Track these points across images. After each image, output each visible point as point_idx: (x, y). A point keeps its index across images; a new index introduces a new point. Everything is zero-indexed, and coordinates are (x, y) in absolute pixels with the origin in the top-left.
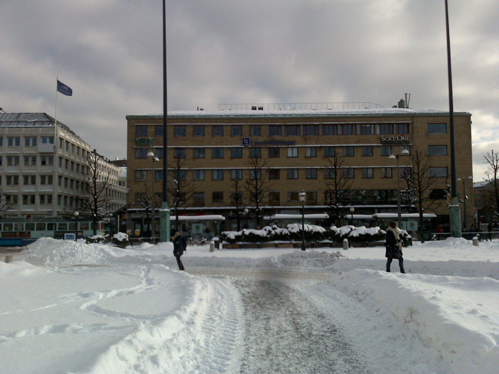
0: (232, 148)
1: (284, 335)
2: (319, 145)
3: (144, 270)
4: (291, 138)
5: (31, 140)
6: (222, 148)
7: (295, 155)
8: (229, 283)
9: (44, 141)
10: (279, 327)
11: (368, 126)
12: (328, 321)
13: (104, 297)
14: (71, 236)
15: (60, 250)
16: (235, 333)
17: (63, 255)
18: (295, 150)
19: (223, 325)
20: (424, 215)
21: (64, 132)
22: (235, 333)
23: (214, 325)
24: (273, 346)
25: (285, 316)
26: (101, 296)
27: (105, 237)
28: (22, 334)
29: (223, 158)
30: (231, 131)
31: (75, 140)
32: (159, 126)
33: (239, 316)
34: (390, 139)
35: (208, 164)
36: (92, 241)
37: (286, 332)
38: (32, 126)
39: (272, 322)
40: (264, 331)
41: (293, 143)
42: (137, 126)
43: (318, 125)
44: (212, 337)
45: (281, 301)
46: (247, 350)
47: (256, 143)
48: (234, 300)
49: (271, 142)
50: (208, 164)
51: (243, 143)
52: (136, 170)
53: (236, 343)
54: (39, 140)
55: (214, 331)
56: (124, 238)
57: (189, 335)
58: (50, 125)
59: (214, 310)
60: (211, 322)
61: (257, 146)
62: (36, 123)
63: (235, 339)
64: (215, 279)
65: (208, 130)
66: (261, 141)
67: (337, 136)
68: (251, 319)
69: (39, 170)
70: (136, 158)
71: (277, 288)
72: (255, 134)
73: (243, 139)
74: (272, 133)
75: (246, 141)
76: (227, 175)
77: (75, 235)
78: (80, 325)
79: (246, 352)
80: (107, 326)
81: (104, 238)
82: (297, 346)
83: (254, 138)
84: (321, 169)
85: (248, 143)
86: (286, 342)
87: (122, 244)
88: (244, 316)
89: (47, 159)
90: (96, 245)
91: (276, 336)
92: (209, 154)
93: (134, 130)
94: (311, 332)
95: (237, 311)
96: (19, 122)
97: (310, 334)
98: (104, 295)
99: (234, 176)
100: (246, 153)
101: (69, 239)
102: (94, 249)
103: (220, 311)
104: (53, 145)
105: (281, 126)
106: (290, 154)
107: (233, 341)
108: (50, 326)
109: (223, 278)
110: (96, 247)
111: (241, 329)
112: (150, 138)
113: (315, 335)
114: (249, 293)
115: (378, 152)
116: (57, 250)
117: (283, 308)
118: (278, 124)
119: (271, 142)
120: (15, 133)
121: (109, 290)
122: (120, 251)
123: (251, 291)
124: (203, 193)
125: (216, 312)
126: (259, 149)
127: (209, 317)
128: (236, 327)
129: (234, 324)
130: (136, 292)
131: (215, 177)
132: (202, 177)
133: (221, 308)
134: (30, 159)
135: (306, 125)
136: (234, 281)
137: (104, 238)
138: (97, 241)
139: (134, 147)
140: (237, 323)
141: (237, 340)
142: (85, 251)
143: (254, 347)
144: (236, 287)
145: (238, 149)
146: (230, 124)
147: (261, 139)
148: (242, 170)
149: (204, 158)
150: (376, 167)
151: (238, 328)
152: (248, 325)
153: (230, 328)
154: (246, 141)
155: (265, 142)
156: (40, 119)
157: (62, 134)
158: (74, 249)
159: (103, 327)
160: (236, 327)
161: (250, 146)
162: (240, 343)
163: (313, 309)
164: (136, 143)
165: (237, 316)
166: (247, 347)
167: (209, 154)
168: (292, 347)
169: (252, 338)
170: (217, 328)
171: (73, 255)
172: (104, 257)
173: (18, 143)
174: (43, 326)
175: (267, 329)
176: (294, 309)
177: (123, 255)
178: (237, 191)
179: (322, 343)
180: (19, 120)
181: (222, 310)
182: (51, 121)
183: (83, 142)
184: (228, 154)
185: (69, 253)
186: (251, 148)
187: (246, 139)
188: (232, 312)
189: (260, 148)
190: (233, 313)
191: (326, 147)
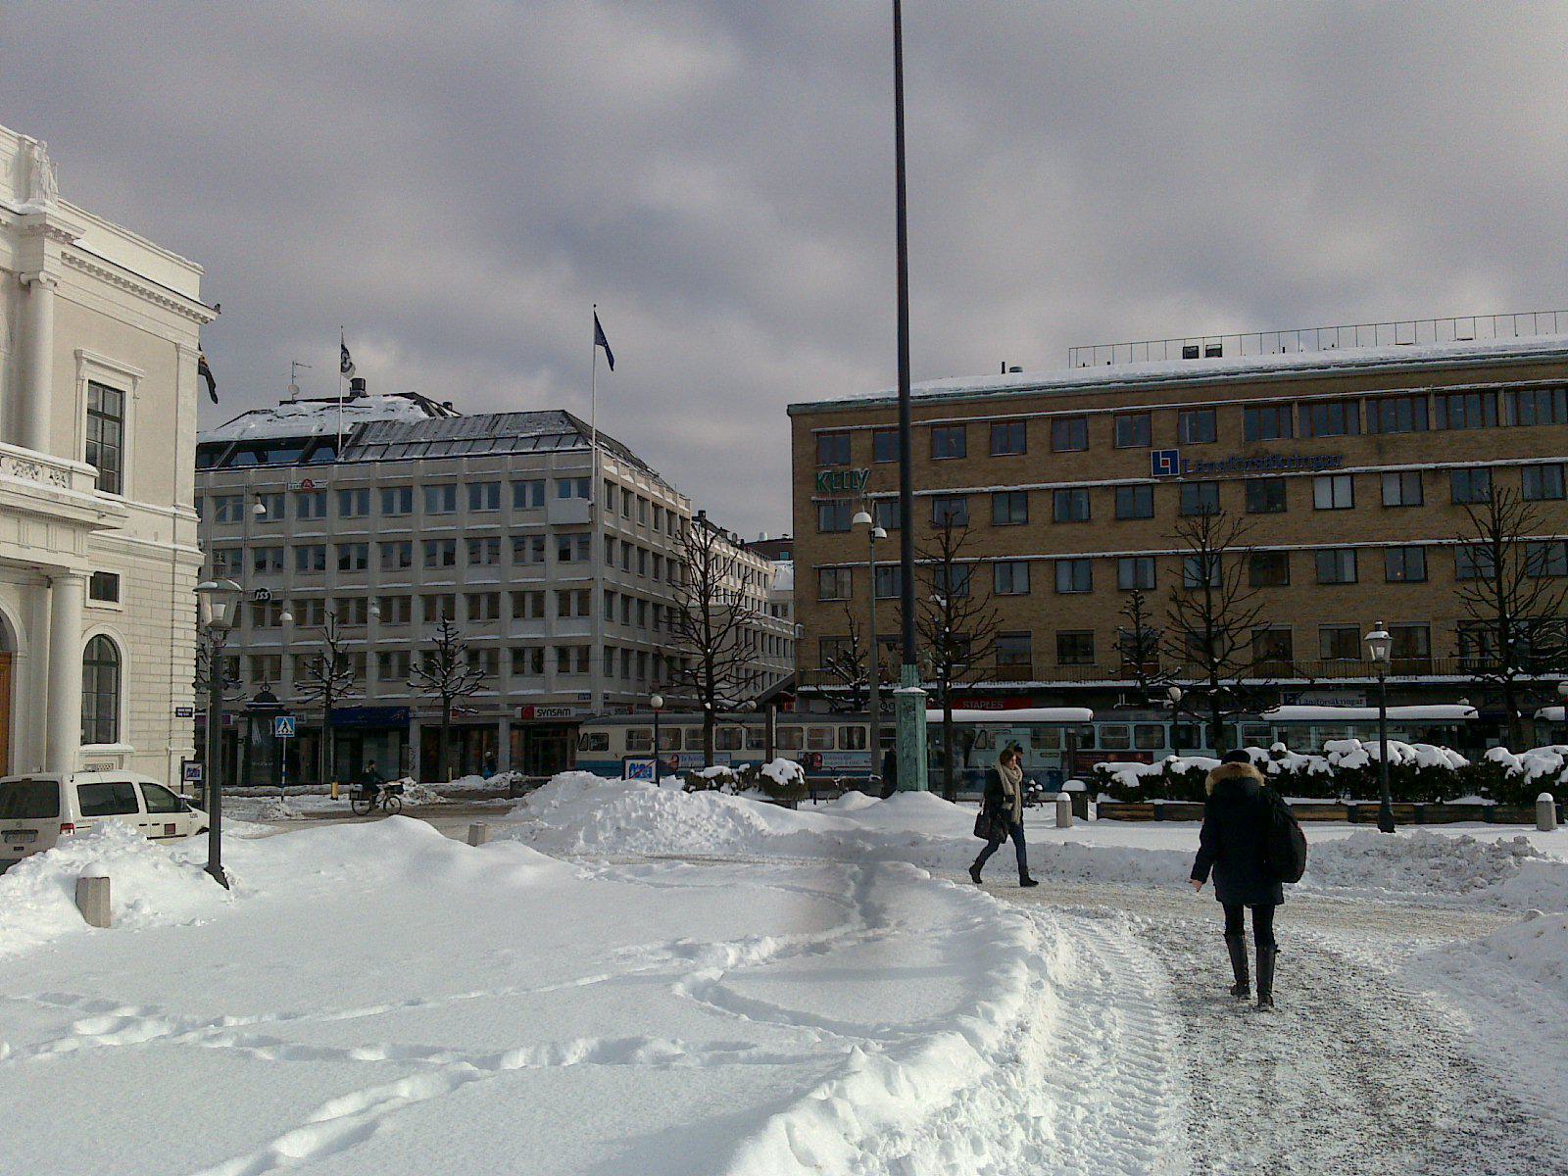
0: (1117, 487)
1: (1329, 1124)
2: (1432, 466)
3: (853, 877)
4: (1325, 445)
5: (530, 491)
6: (1086, 488)
8: (1126, 933)
9: (564, 493)
10: (1309, 1094)
12: (1490, 1084)
13: (740, 960)
14: (643, 766)
15: (615, 808)
16: (1155, 1104)
17: (623, 824)
18: (1343, 487)
19: (1114, 1073)
21: (615, 464)
22: (1155, 1104)
23: (1085, 1070)
24: (1290, 1158)
25: (1329, 1057)
26: (732, 955)
27: (738, 773)
28: (517, 1061)
29: (1088, 520)
30: (1114, 429)
31: (648, 485)
33: (1166, 1046)
35: (1039, 542)
36: (701, 784)
37: (1334, 1111)
38: (531, 450)
39: (1281, 1072)
40: (1256, 1103)
41: (1335, 460)
42: (819, 434)
43: (1425, 395)
44: (1080, 1113)
45: (1312, 1004)
46: (1199, 1164)
47: (1200, 467)
48: (1147, 994)
49: (1255, 463)
50: (1039, 542)
51: (1157, 469)
52: (820, 569)
53: (1162, 1136)
54: (551, 490)
55: (1085, 1092)
56: (791, 778)
57: (1004, 1099)
58: (580, 446)
59: (1082, 1024)
60: (1073, 1061)
61: (1204, 478)
62: (541, 439)
63: (1158, 1125)
64: (1081, 920)
65: (1038, 434)
66: (1218, 460)
67: (1493, 431)
68: (1209, 1060)
69: (554, 574)
70: (820, 533)
71: (1293, 959)
72: (1196, 437)
73: (1156, 455)
74: (1254, 433)
76: (1103, 577)
77: (654, 765)
78: (674, 1042)
79: (1198, 1170)
80: (754, 1051)
81: (736, 777)
82: (1378, 1164)
83: (1191, 452)
85: (1174, 470)
86: (1338, 1149)
87: (785, 795)
88: (1185, 1048)
89: (572, 542)
90: (715, 795)
91: (1300, 1125)
92: (1040, 510)
93: (811, 449)
94: (1428, 1118)
95: (1160, 1029)
96: (496, 439)
97: (1425, 1126)
98: (741, 950)
99: (1127, 579)
100: (1166, 501)
101: (637, 776)
102: (706, 807)
103: (1100, 1025)
104: (590, 502)
105: (1289, 404)
106: (1323, 500)
107: (1153, 1131)
108: (594, 1042)
109: (1106, 916)
110: (712, 803)
111: (1176, 1093)
112: (859, 470)
113: (1444, 1133)
114: (1196, 971)
116: (606, 812)
117: (1319, 1029)
118: (1276, 399)
119: (1255, 463)
120: (487, 470)
121: (756, 936)
122: (783, 816)
123: (1203, 966)
125: (1086, 1028)
126: (1212, 487)
127: (1068, 1044)
128: (1158, 1083)
129: (1151, 1074)
130: (834, 946)
131: (1064, 583)
132: (1020, 583)
133: (1105, 1016)
134: (527, 545)
135: (1379, 398)
136: (1144, 926)
137: (736, 777)
138: (714, 784)
139: (813, 498)
140: (1163, 1070)
141: (1163, 1129)
142: (682, 815)
143: (1224, 1157)
144: (1153, 949)
145: (1138, 491)
146: (1112, 410)
147: (1217, 453)
148: (1154, 557)
151: (1164, 1086)
152: (1199, 1078)
153: (1139, 1087)
155: (1232, 464)
156: (552, 430)
157: (610, 468)
158: (652, 808)
159: (742, 1054)
160: (1158, 1083)
162: (1174, 1139)
163: (1433, 1037)
164: (819, 487)
165: (1160, 1046)
166: (1200, 1153)
167: (1040, 510)
168: (1360, 1167)
169: (1217, 1125)
170: (1094, 1084)
171: (648, 824)
172: (735, 832)
173: (494, 502)
174: (574, 1040)
175: (1268, 1100)
176: (1363, 1034)
177: (790, 829)
178: (1138, 629)
179: (1474, 1162)
180: (496, 432)
181: (1107, 1024)
182: (582, 432)
183: (669, 489)
184: (1104, 508)
185: (640, 818)
186: (1182, 483)
187: (1165, 454)
188: (1142, 1033)
189: (1217, 482)
190: (1148, 1036)
191: (1454, 468)
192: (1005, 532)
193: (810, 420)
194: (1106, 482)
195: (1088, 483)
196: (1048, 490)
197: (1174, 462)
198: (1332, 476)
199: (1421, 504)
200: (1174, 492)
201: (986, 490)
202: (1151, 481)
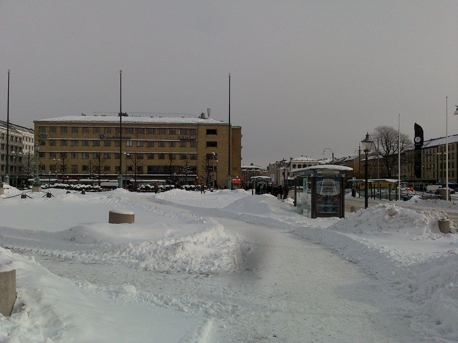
0: (94, 140)
2: (145, 140)
4: (129, 135)
7: (131, 145)
11: (173, 129)
18: (131, 142)
20: (137, 181)
32: (52, 127)
34: (185, 138)
41: (129, 138)
42: (39, 127)
43: (144, 128)
47: (108, 138)
50: (80, 149)
51: (100, 138)
65: (80, 130)
67: (155, 135)
75: (102, 136)
84: (145, 153)
85: (103, 138)
100: (102, 143)
106: (128, 145)
115: (178, 145)
124: (77, 166)
135: (138, 128)
147: (111, 136)
149: (77, 146)
150: (177, 153)
154: (102, 136)
155: (113, 137)
161: (104, 139)
167: (80, 143)
192: (74, 147)
193: (38, 124)
194: (91, 139)
195: (88, 139)
196: (81, 140)
197: (100, 136)
198: (129, 141)
199: (143, 146)
200: (104, 142)
201: (70, 139)
202: (99, 139)
